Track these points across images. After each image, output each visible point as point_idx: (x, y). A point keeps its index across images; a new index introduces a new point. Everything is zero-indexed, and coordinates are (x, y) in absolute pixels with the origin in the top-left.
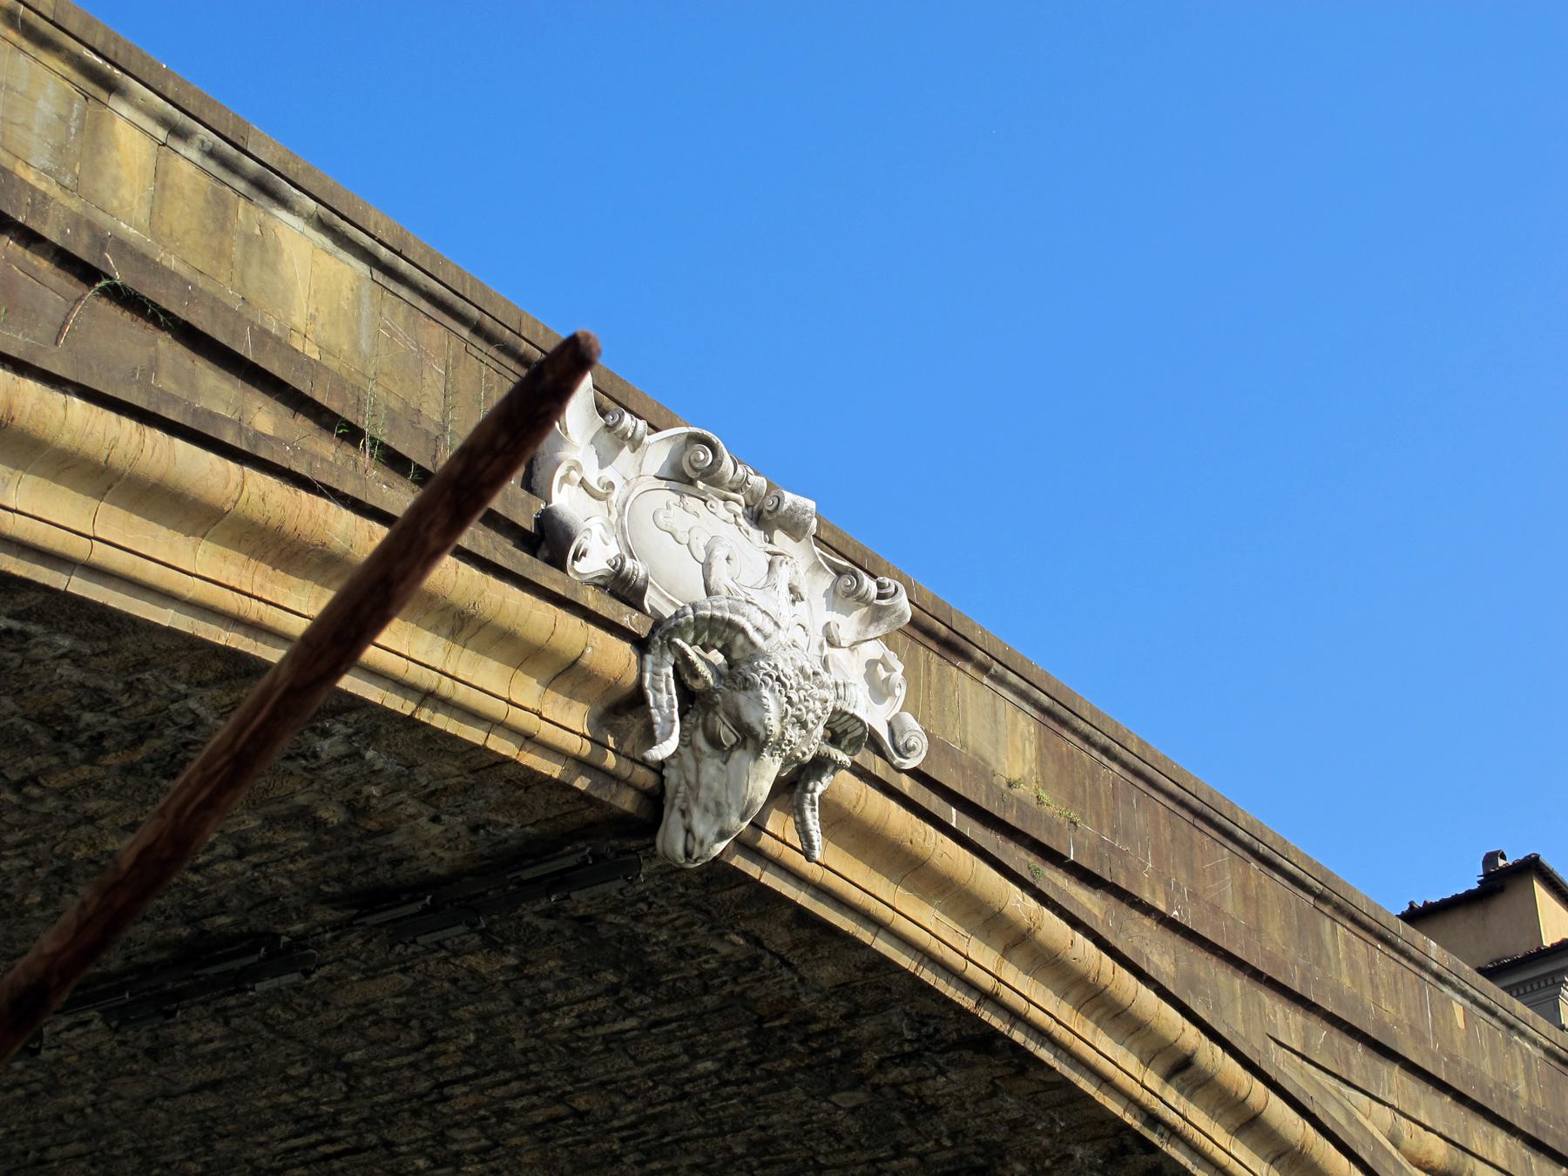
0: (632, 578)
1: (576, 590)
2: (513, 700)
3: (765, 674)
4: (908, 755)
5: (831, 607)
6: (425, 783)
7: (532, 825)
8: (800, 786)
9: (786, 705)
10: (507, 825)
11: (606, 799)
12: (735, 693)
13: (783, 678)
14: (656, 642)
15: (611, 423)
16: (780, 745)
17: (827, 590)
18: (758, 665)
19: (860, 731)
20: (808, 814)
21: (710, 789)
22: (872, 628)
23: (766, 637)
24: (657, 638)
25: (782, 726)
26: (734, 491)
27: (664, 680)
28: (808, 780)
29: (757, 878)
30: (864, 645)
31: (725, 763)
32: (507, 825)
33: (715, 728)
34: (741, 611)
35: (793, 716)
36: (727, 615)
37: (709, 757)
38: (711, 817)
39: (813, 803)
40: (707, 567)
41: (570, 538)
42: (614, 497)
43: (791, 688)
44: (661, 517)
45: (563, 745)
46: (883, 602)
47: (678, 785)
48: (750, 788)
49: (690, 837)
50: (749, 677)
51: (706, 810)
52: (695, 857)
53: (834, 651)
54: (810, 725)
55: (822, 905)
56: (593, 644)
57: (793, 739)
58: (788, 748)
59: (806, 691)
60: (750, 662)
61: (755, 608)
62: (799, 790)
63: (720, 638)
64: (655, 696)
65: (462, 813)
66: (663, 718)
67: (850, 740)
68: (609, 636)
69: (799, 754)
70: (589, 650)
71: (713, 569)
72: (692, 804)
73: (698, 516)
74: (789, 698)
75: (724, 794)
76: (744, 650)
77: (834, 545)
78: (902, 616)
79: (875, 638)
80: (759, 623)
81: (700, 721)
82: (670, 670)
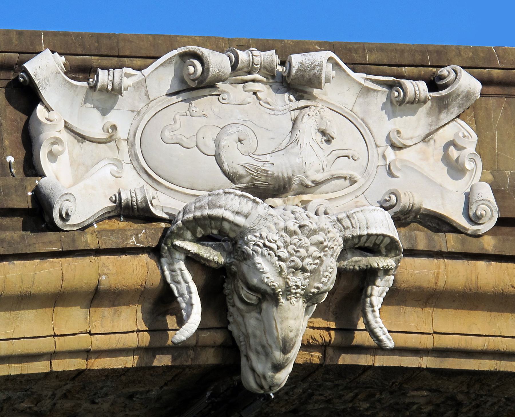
0: (132, 205)
1: (74, 241)
2: (58, 333)
3: (254, 245)
4: (481, 222)
5: (392, 115)
6: (50, 393)
7: (166, 384)
8: (364, 293)
9: (277, 263)
10: (148, 391)
11: (189, 363)
12: (241, 263)
13: (267, 243)
14: (164, 249)
15: (92, 84)
16: (290, 291)
17: (384, 104)
18: (247, 238)
19: (387, 241)
20: (370, 316)
21: (255, 336)
22: (443, 116)
23: (246, 216)
24: (163, 245)
25: (284, 278)
26: (249, 73)
27: (179, 272)
28: (368, 285)
29: (371, 364)
30: (441, 131)
31: (260, 313)
32: (148, 391)
33: (239, 291)
34: (218, 204)
35: (289, 268)
36: (206, 212)
37: (247, 312)
38: (263, 358)
39: (372, 306)
40: (218, 157)
41: (51, 208)
42: (122, 133)
43: (279, 248)
44: (167, 134)
45: (121, 346)
46: (444, 92)
47: (239, 337)
48: (279, 330)
49: (256, 376)
50: (244, 250)
51: (258, 353)
52: (266, 387)
53: (403, 154)
54: (309, 268)
55: (450, 360)
56: (106, 271)
57: (299, 284)
58: (299, 290)
59: (295, 244)
60: (243, 238)
61: (232, 196)
62: (363, 296)
63: (212, 228)
64: (177, 288)
65: (106, 395)
66: (186, 304)
67: (386, 247)
68: (124, 257)
69: (315, 291)
70: (104, 278)
71: (223, 158)
72: (248, 350)
73: (206, 116)
74: (279, 256)
75: (264, 338)
76: (234, 231)
77: (385, 61)
78: (468, 95)
79: (453, 120)
80: (236, 208)
81: (233, 287)
82: (182, 265)
